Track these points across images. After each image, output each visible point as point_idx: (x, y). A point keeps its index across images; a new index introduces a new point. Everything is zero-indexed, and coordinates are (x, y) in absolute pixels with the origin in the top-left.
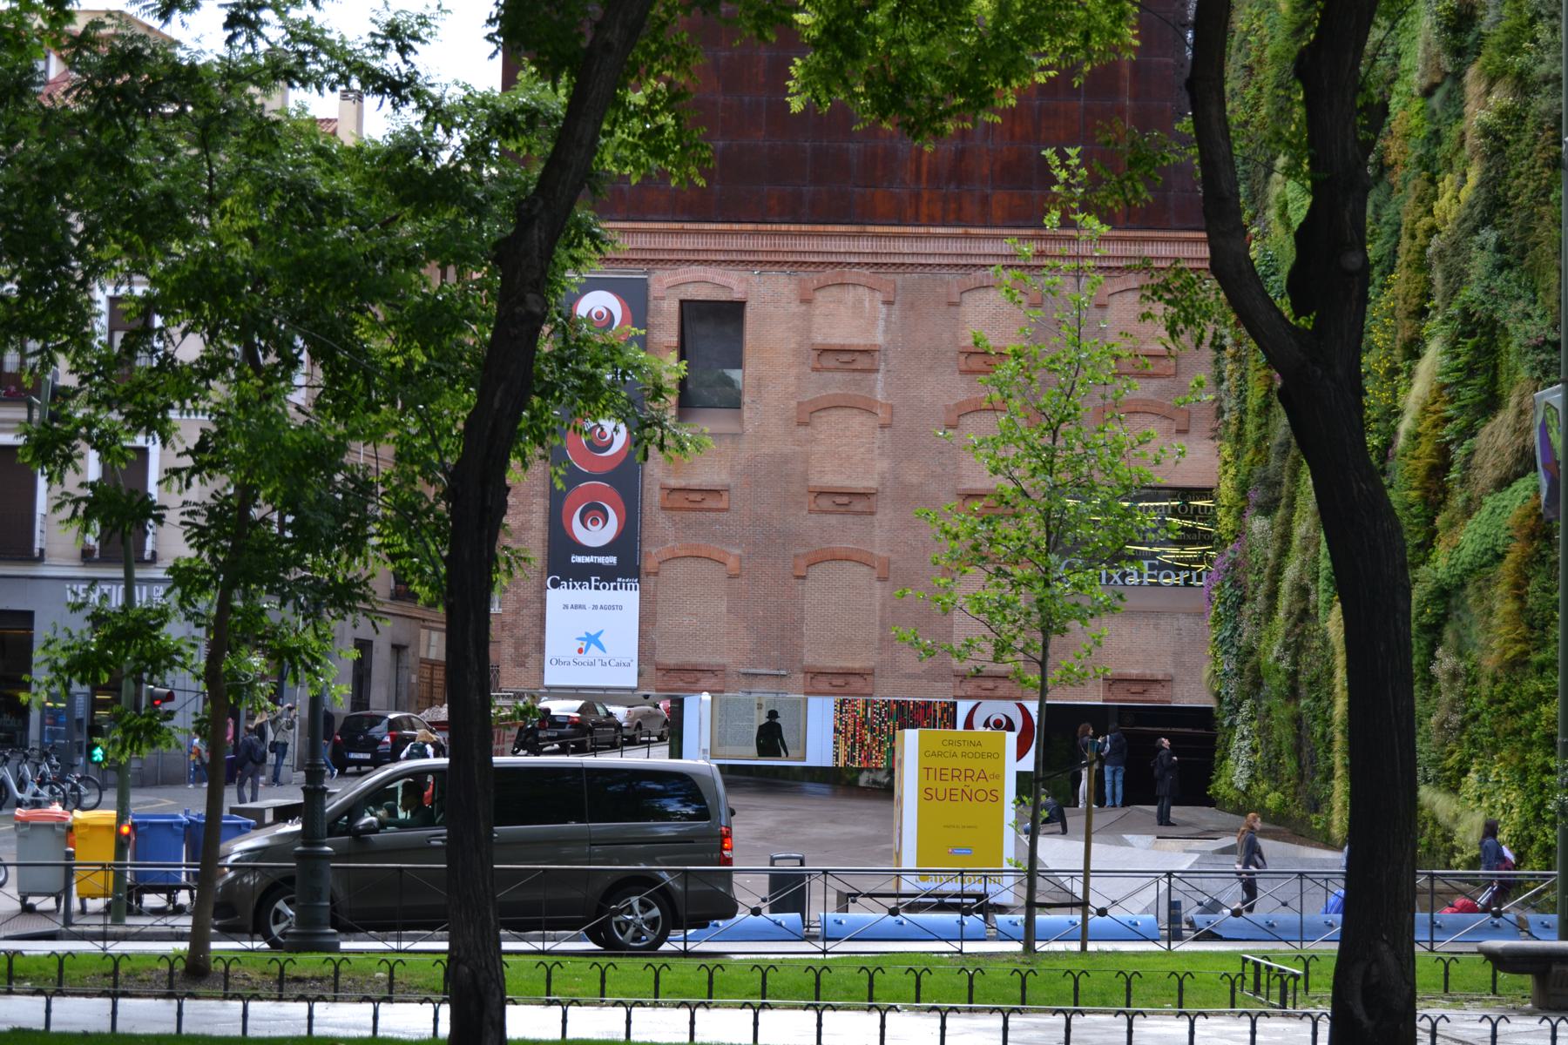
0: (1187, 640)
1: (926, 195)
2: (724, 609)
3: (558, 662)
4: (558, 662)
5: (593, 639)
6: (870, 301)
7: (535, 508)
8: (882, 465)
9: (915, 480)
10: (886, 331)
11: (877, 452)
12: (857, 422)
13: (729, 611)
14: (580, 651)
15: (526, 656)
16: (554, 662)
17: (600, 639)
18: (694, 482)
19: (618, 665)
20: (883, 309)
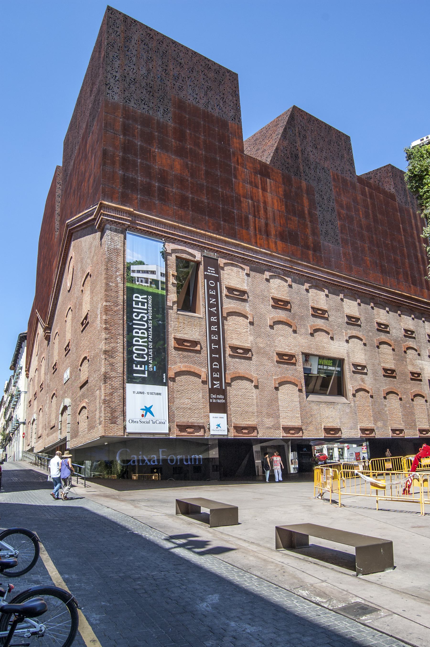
0: (342, 413)
1: (258, 236)
2: (201, 396)
3: (133, 421)
4: (133, 421)
5: (148, 410)
6: (242, 274)
7: (119, 341)
8: (251, 338)
9: (261, 345)
10: (248, 284)
11: (249, 332)
12: (241, 319)
13: (203, 398)
14: (143, 416)
15: (117, 418)
16: (131, 421)
17: (151, 409)
18: (186, 337)
19: (160, 423)
20: (246, 277)
